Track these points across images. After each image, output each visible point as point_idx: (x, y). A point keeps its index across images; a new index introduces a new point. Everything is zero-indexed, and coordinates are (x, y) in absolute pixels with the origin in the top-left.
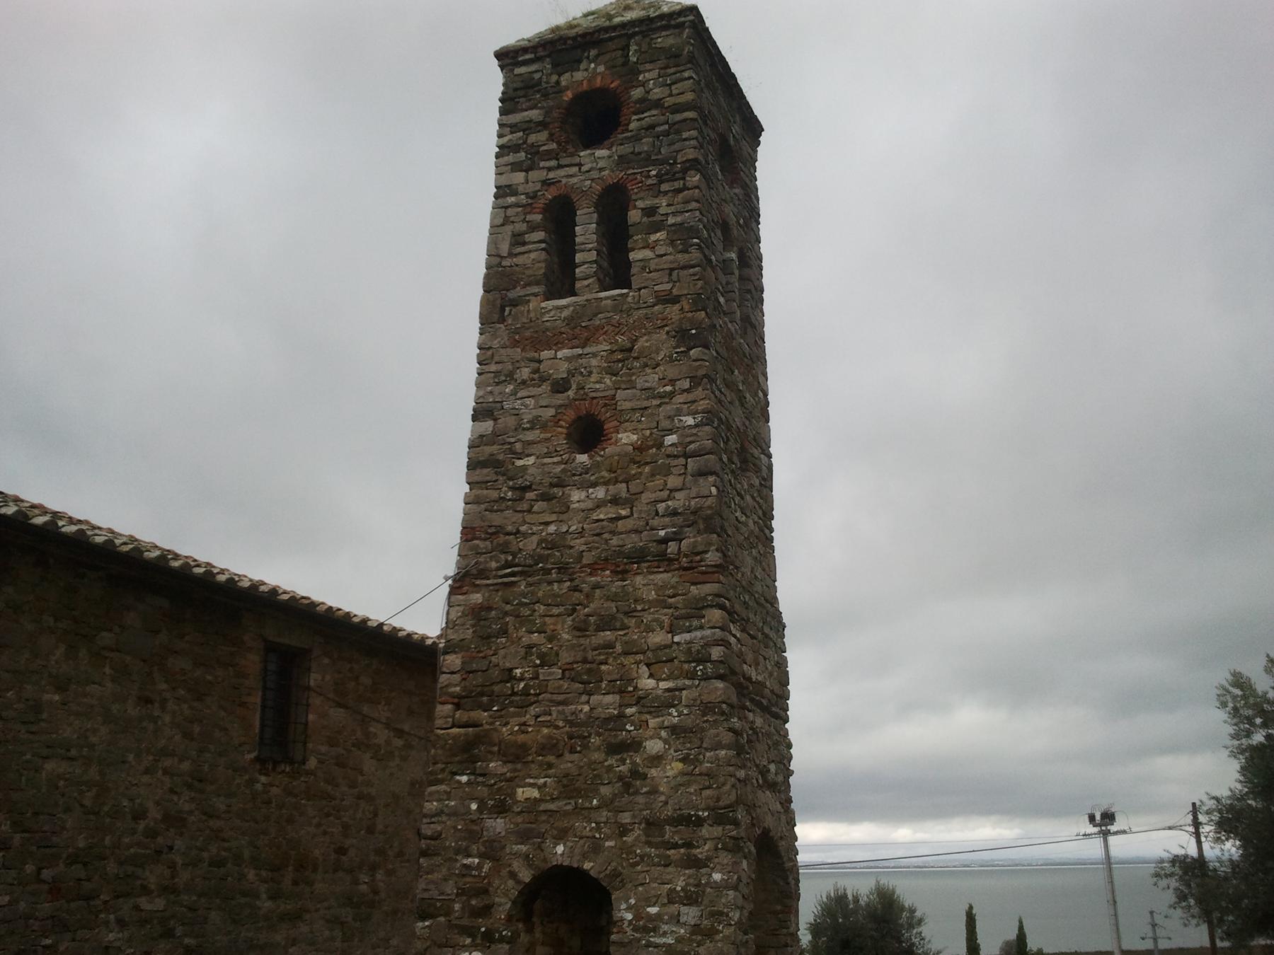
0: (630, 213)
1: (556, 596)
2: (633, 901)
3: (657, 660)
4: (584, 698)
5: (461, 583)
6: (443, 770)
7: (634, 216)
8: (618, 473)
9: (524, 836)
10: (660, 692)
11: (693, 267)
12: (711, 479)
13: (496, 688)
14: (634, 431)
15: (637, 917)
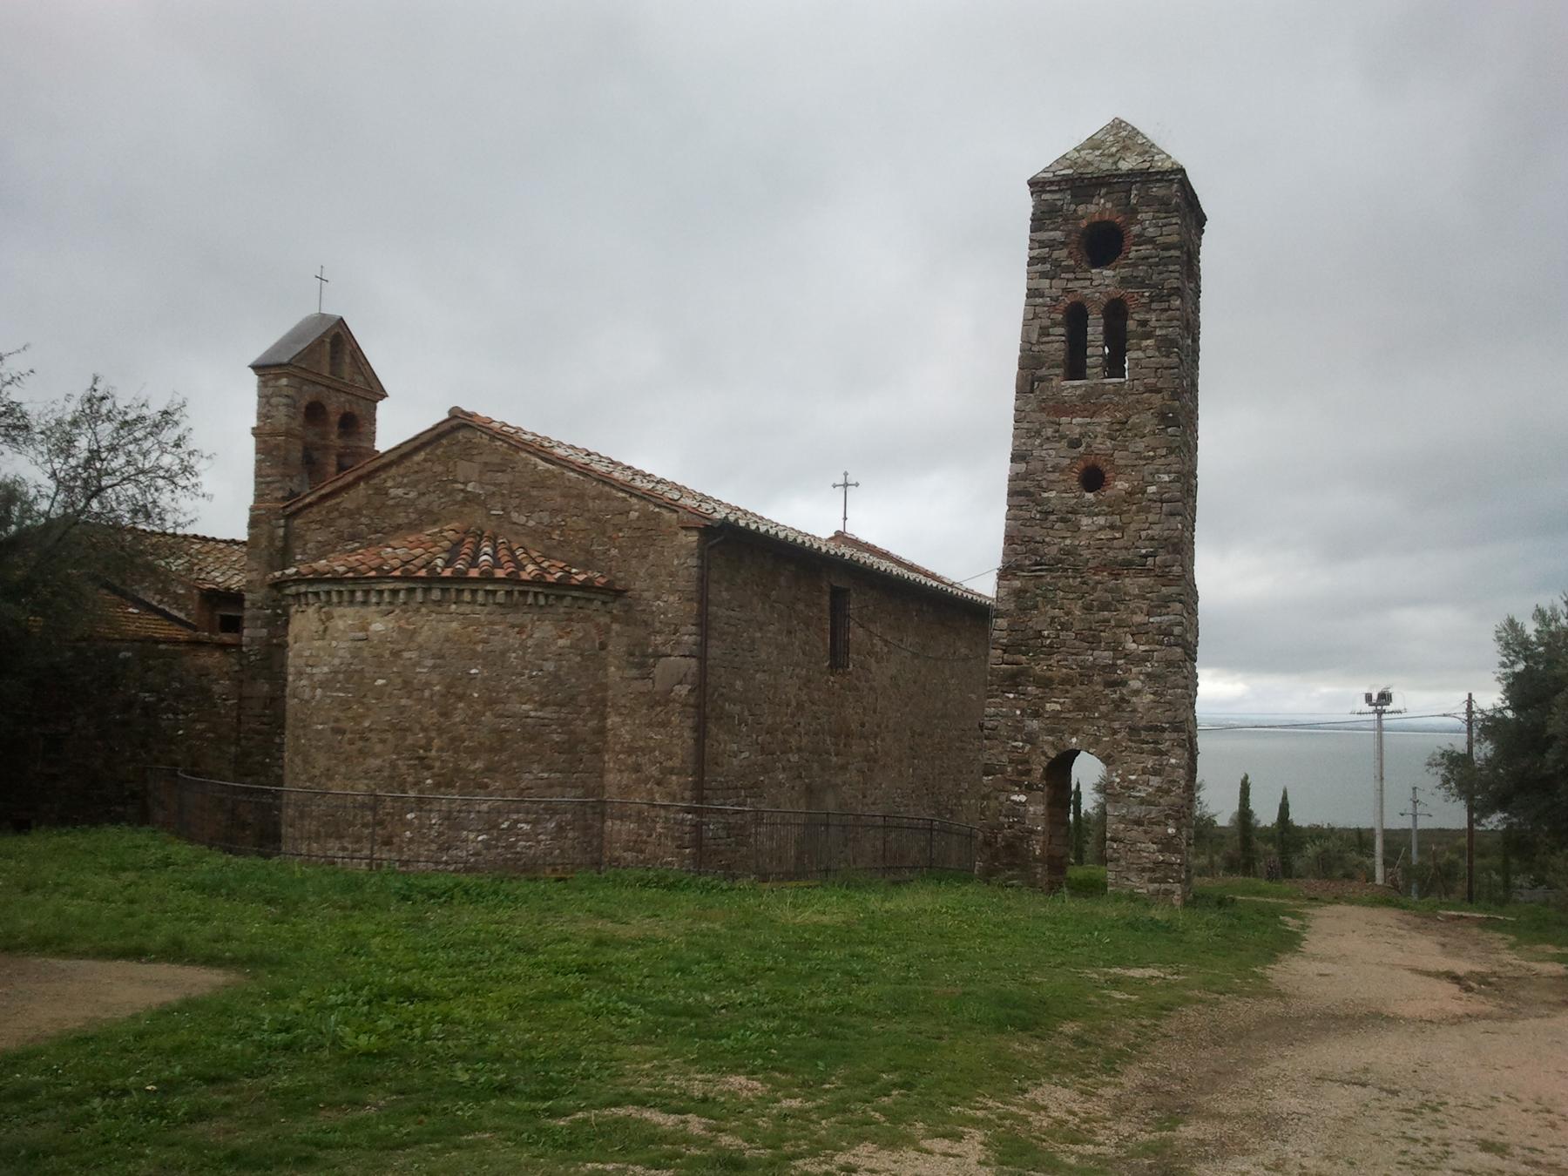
0: (1128, 322)
1: (1071, 586)
2: (1120, 772)
3: (1138, 633)
4: (1090, 652)
5: (1005, 574)
6: (997, 690)
7: (1131, 325)
8: (1114, 507)
9: (1051, 732)
11: (1173, 368)
12: (1179, 518)
14: (1127, 481)
15: (1123, 780)
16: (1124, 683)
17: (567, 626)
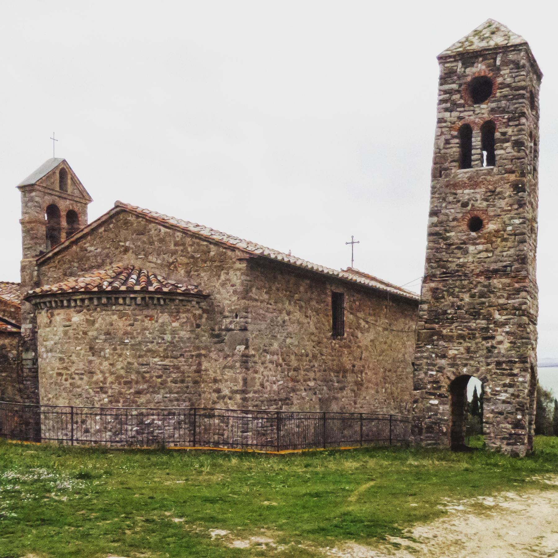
3: (502, 308)
4: (474, 321)
10: (502, 320)
13: (441, 317)
15: (493, 391)
16: (493, 338)
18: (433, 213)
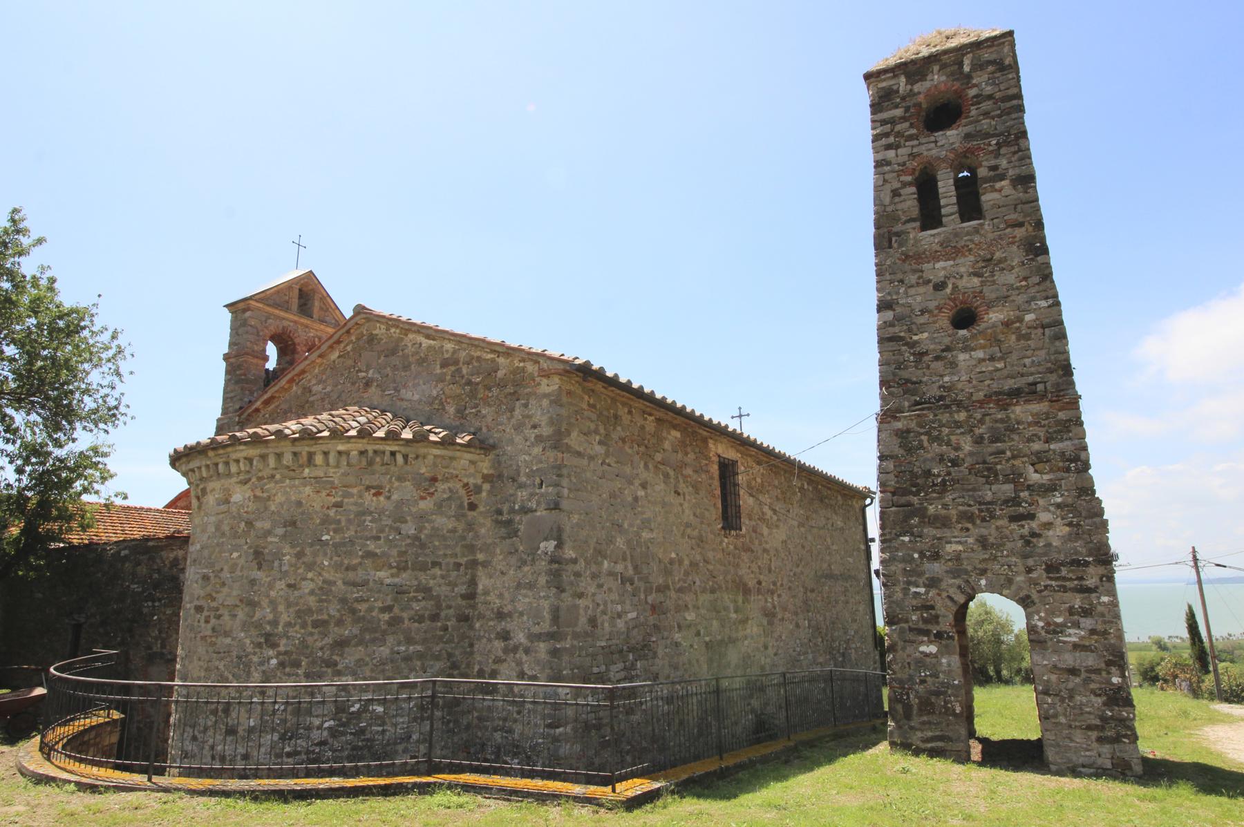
1: (956, 422)
2: (1042, 614)
3: (1039, 460)
4: (988, 486)
9: (955, 573)
15: (1048, 624)
16: (1032, 517)
17: (430, 486)
18: (883, 306)
